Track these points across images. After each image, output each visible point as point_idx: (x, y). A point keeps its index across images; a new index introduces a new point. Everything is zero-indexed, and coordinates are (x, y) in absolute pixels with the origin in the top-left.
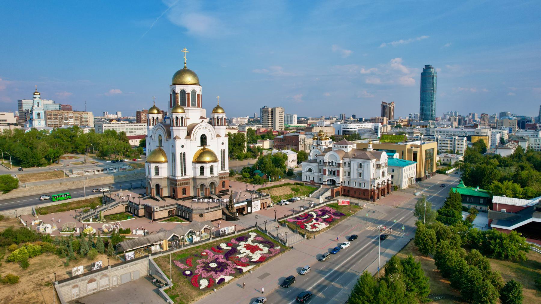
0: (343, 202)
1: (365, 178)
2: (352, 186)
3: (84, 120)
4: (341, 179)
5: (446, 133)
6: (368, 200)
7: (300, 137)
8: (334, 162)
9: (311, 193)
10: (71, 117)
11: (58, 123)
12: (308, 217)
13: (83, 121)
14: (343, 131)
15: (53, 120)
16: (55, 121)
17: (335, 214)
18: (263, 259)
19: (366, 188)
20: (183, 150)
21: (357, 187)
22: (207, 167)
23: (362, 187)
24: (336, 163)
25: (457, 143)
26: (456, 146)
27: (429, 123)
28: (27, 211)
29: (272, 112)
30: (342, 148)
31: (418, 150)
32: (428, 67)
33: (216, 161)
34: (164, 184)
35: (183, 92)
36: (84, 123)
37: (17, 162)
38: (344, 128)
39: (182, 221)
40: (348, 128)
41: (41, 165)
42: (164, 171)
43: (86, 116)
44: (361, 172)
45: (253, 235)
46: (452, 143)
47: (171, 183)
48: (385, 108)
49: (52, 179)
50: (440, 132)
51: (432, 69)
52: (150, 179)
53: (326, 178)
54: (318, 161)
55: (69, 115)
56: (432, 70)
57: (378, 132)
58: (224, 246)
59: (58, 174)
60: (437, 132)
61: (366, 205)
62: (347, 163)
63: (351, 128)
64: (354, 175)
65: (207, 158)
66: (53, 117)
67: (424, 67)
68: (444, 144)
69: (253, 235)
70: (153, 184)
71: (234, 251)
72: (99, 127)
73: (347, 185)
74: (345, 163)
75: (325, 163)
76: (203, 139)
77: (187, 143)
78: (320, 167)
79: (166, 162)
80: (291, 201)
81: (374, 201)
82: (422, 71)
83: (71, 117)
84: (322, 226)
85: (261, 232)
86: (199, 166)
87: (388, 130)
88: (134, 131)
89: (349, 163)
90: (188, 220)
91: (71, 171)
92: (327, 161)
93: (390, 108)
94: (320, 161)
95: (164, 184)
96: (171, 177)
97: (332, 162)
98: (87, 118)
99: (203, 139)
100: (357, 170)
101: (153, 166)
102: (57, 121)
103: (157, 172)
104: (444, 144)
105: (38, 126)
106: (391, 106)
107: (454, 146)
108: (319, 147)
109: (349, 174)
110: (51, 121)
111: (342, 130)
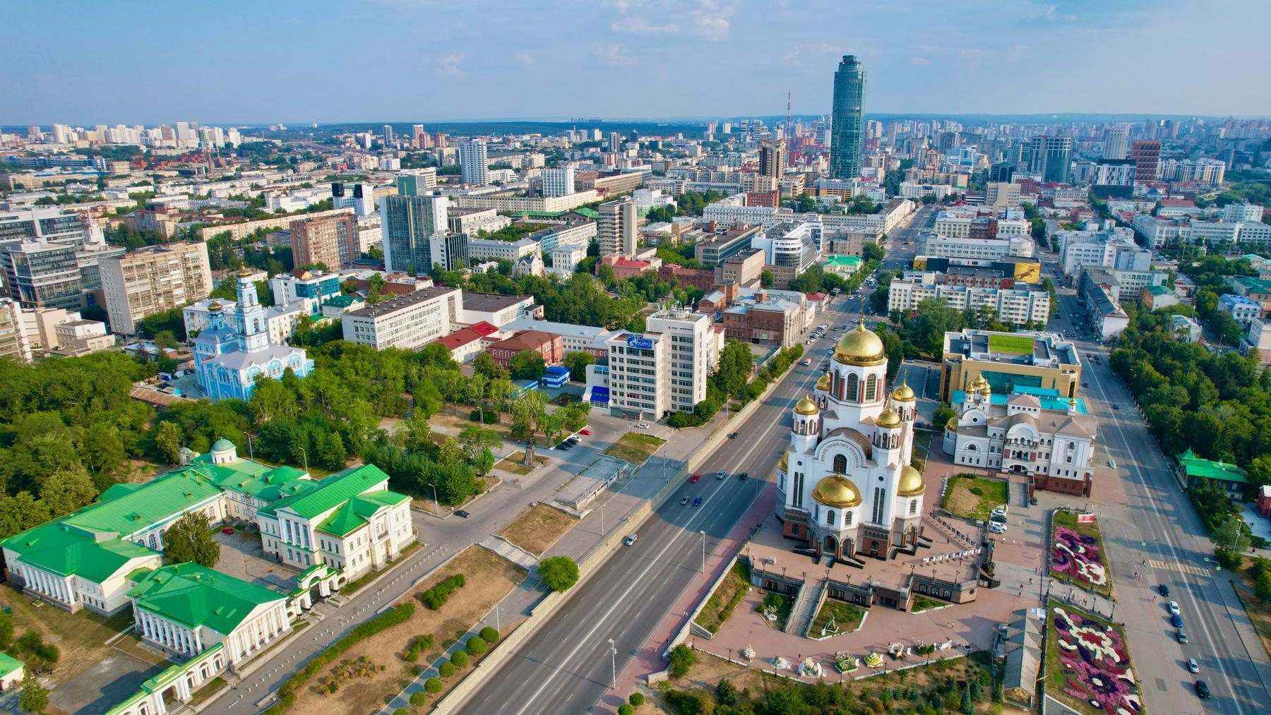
0: (1084, 519)
1: (1078, 464)
2: (1053, 474)
3: (190, 265)
5: (956, 249)
6: (1079, 495)
8: (1026, 439)
11: (148, 287)
13: (189, 269)
14: (777, 254)
15: (137, 282)
16: (141, 282)
19: (1077, 478)
21: (1062, 475)
23: (1070, 477)
24: (1029, 441)
25: (1035, 303)
26: (1035, 308)
29: (620, 214)
30: (1027, 412)
32: (849, 61)
36: (192, 273)
38: (778, 249)
39: (944, 605)
40: (787, 249)
42: (861, 514)
43: (194, 255)
44: (1070, 454)
46: (1028, 302)
47: (866, 533)
49: (560, 531)
50: (947, 246)
52: (838, 533)
53: (1008, 463)
54: (990, 433)
55: (170, 263)
56: (859, 68)
57: (819, 243)
60: (940, 246)
62: (1046, 441)
63: (793, 249)
64: (1058, 459)
66: (135, 273)
67: (842, 60)
68: (1013, 304)
70: (841, 539)
72: (358, 325)
73: (1041, 472)
74: (1042, 440)
75: (1006, 441)
78: (993, 443)
79: (857, 501)
81: (1088, 496)
86: (910, 500)
88: (418, 320)
89: (1050, 441)
90: (948, 599)
92: (1013, 437)
94: (995, 434)
96: (870, 525)
97: (1023, 440)
98: (195, 259)
100: (1065, 452)
102: (146, 281)
103: (849, 518)
104: (1013, 304)
105: (257, 350)
107: (1031, 307)
108: (980, 407)
109: (1048, 456)
110: (133, 283)
111: (774, 252)
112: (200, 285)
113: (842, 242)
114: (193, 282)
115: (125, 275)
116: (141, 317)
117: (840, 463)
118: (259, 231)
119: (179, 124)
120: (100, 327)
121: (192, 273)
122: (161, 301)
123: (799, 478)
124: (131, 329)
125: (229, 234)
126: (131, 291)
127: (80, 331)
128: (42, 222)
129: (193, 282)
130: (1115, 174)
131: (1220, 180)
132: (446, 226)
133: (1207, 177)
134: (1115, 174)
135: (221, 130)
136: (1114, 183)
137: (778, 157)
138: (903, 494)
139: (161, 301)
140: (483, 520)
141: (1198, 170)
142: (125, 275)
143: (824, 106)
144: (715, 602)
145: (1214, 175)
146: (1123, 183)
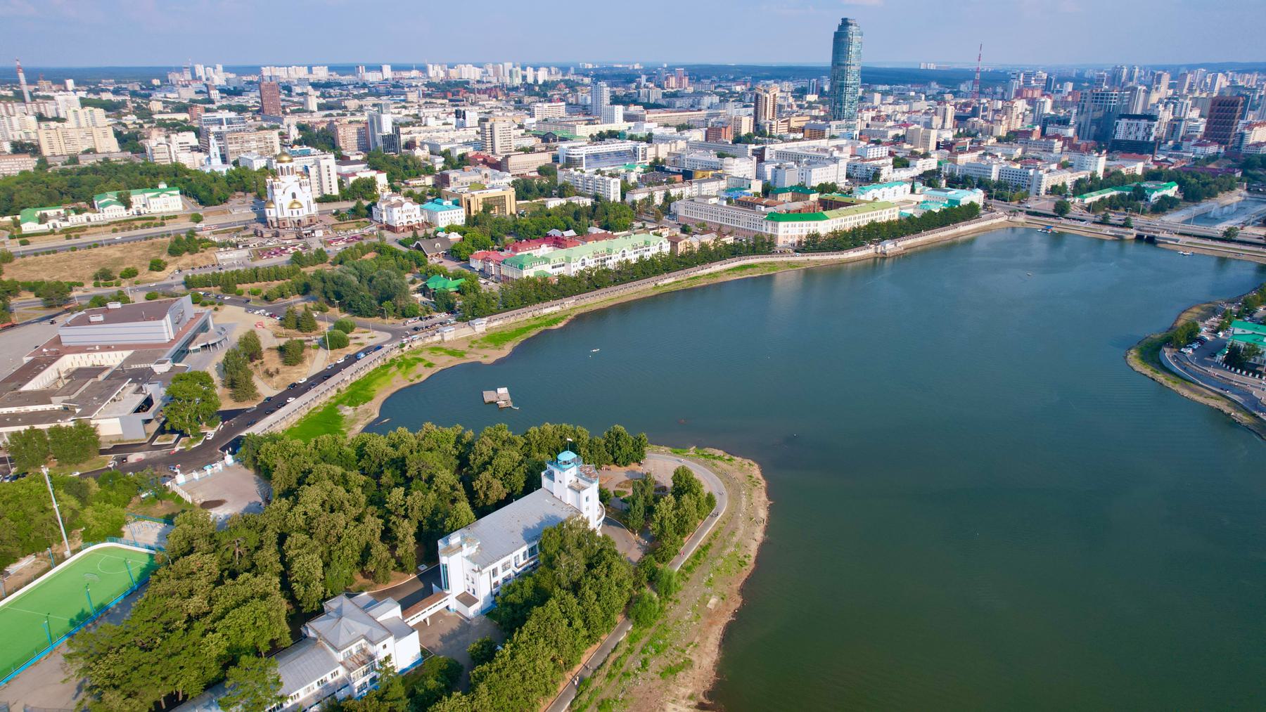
3: (268, 141)
7: (450, 176)
10: (253, 140)
15: (234, 145)
20: (280, 202)
22: (295, 211)
27: (830, 127)
28: (208, 233)
32: (845, 23)
33: (302, 207)
34: (274, 220)
37: (202, 203)
41: (216, 205)
48: (759, 98)
51: (850, 27)
59: (224, 212)
65: (296, 206)
66: (233, 141)
76: (294, 196)
77: (282, 197)
82: (836, 30)
83: (253, 140)
87: (678, 148)
93: (766, 98)
95: (274, 220)
98: (270, 139)
99: (294, 196)
106: (767, 95)
114: (269, 149)
115: (228, 141)
119: (505, 64)
121: (269, 145)
128: (227, 119)
129: (269, 149)
130: (1133, 129)
134: (1133, 129)
135: (532, 69)
136: (1132, 138)
137: (766, 101)
142: (228, 141)
143: (824, 58)
146: (1140, 139)
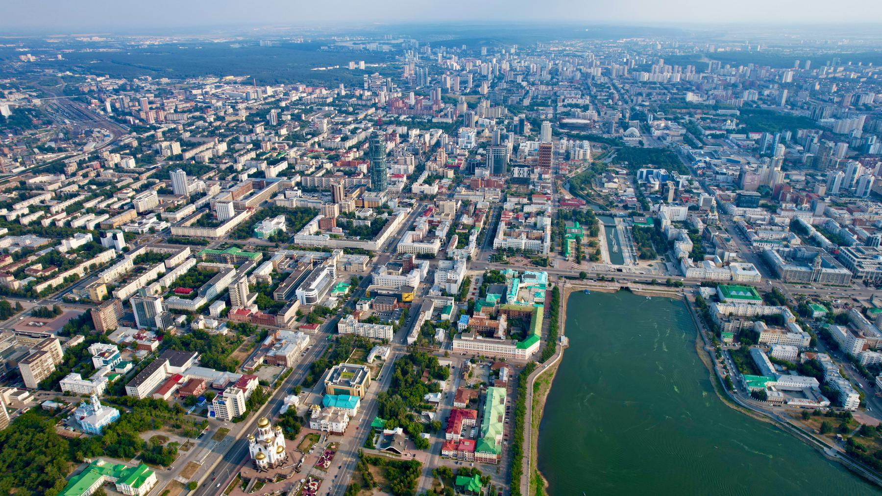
3: (53, 350)
4: (328, 430)
9: (318, 440)
12: (322, 460)
17: (331, 453)
18: (318, 488)
31: (360, 389)
35: (265, 431)
36: (54, 353)
42: (266, 460)
45: (310, 478)
53: (323, 429)
58: (305, 487)
61: (341, 440)
69: (310, 478)
71: (309, 488)
80: (313, 449)
84: (329, 463)
85: (312, 476)
91: (199, 461)
101: (261, 461)
112: (58, 355)
113: (349, 266)
116: (39, 381)
117: (260, 450)
118: (65, 279)
120: (27, 394)
121: (54, 353)
122: (46, 372)
123: (253, 452)
124: (36, 386)
125: (50, 286)
126: (34, 374)
127: (20, 398)
130: (522, 172)
131: (588, 157)
132: (161, 310)
133: (581, 157)
134: (522, 172)
136: (521, 176)
138: (278, 453)
139: (46, 372)
140: (175, 470)
141: (577, 153)
144: (230, 487)
145: (585, 155)
